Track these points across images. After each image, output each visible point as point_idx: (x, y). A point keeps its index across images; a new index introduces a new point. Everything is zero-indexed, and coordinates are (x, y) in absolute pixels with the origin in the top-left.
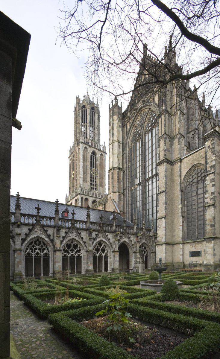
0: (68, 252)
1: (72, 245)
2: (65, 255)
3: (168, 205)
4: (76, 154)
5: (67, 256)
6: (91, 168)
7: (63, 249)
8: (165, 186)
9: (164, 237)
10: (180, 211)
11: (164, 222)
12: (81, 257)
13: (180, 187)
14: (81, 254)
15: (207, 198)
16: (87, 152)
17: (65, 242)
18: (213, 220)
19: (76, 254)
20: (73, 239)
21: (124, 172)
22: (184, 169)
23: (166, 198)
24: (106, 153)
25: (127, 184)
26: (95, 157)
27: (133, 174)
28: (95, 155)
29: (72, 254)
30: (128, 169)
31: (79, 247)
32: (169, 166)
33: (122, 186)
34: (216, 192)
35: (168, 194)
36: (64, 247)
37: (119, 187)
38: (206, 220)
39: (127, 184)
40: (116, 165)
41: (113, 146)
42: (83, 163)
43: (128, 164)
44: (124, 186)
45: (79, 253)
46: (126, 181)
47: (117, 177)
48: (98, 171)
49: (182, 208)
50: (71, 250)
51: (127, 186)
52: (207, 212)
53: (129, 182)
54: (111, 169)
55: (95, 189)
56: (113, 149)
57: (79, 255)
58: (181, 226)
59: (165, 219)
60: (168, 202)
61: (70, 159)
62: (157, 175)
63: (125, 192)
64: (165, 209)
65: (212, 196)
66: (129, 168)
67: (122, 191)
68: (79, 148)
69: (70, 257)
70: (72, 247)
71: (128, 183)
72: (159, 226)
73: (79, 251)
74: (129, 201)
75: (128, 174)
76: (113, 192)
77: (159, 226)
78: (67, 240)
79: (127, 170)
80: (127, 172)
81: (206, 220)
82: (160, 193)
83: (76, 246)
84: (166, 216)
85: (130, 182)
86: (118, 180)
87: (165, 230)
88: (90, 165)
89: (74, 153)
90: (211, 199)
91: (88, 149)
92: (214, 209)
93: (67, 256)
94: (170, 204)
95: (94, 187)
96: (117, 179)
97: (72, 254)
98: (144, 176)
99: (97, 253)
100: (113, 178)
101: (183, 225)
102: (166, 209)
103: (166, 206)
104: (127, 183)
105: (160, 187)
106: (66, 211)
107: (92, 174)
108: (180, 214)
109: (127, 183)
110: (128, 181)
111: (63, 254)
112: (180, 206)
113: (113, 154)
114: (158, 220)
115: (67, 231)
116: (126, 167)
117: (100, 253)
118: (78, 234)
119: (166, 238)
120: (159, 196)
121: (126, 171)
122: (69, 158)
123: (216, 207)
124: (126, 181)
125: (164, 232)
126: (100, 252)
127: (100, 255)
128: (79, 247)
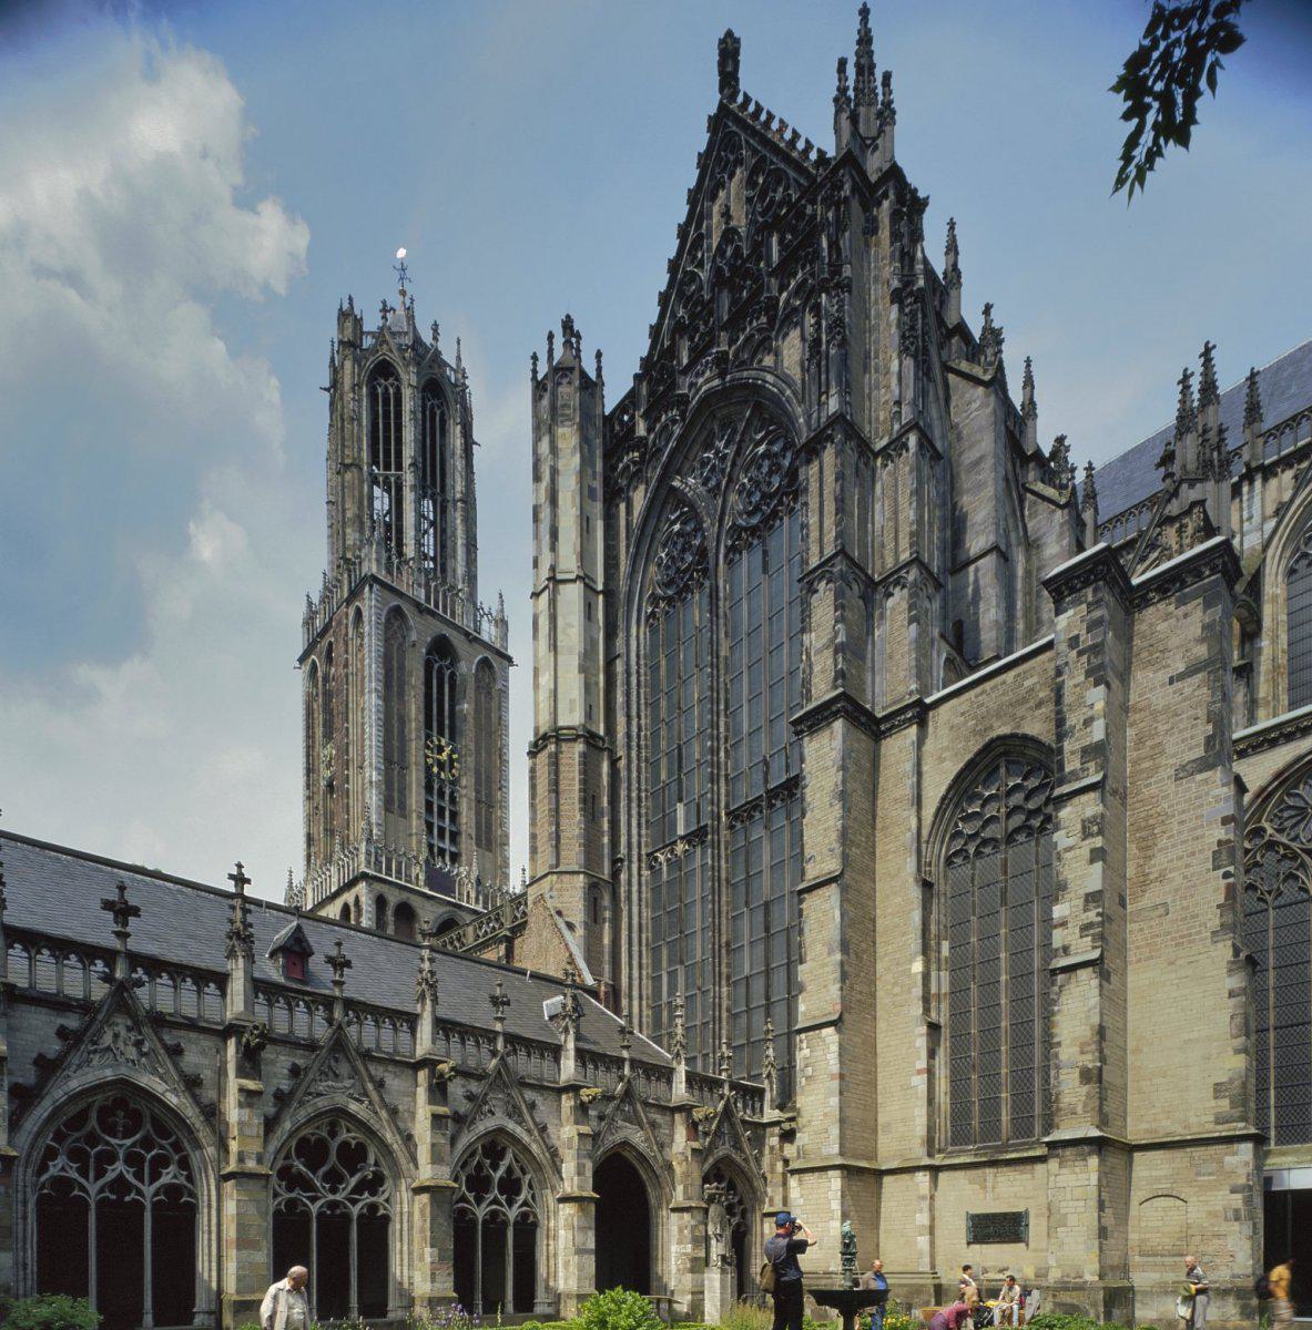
0: (308, 1186)
1: (334, 1145)
2: (291, 1204)
3: (853, 956)
5: (301, 1208)
7: (279, 1164)
8: (838, 851)
9: (835, 1131)
10: (918, 991)
11: (834, 1048)
13: (919, 861)
14: (387, 1201)
15: (1064, 924)
17: (287, 1125)
18: (1093, 1047)
19: (354, 1202)
21: (614, 762)
22: (941, 760)
29: (331, 1197)
30: (639, 746)
31: (376, 1164)
33: (606, 840)
34: (1107, 895)
36: (287, 1157)
38: (1059, 1044)
40: (572, 717)
44: (614, 844)
45: (373, 1193)
47: (577, 787)
49: (926, 976)
50: (326, 1178)
52: (1063, 999)
54: (545, 737)
56: (553, 618)
57: (373, 1207)
58: (919, 1072)
59: (839, 1031)
62: (791, 789)
63: (623, 877)
65: (1092, 916)
69: (320, 1215)
70: (333, 1158)
72: (809, 1071)
73: (374, 1184)
74: (640, 924)
76: (555, 870)
77: (809, 1071)
78: (302, 1115)
79: (634, 754)
81: (1059, 1044)
82: (810, 890)
83: (353, 1156)
84: (846, 1016)
86: (584, 801)
87: (841, 1093)
90: (1085, 928)
92: (1101, 985)
94: (864, 951)
96: (576, 795)
97: (331, 1197)
98: (723, 791)
99: (479, 1200)
101: (930, 1071)
102: (844, 976)
103: (845, 957)
104: (634, 822)
105: (813, 852)
109: (634, 822)
111: (276, 1195)
112: (918, 967)
113: (554, 647)
114: (803, 1036)
115: (300, 1062)
116: (628, 735)
117: (495, 1201)
118: (370, 1086)
119: (842, 1137)
120: (804, 906)
123: (1109, 974)
125: (834, 1101)
126: (490, 1197)
127: (494, 1214)
128: (371, 1160)
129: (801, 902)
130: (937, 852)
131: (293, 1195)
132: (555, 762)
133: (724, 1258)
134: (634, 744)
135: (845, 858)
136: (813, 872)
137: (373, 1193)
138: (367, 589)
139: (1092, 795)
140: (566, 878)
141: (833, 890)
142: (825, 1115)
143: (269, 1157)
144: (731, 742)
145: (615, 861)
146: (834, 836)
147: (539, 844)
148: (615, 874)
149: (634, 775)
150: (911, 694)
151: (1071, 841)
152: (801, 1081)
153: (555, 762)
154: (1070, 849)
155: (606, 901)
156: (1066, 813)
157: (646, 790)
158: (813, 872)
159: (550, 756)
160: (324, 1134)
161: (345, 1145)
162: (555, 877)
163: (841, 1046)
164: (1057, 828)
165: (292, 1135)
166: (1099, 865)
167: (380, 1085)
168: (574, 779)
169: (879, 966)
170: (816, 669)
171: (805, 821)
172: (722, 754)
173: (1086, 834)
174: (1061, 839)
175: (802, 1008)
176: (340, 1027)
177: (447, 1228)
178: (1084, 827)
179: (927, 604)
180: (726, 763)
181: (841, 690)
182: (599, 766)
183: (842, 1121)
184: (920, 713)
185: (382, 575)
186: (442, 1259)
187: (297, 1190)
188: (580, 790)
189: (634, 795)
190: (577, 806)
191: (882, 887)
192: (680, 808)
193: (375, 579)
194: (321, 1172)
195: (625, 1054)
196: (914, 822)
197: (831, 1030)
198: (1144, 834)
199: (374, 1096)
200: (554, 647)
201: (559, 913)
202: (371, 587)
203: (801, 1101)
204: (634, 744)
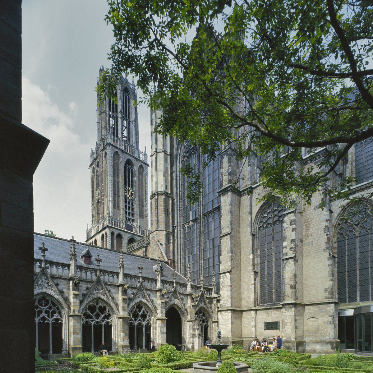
0: (91, 318)
1: (98, 307)
2: (87, 322)
5: (89, 323)
7: (83, 313)
8: (230, 227)
9: (230, 300)
10: (251, 263)
11: (229, 278)
12: (111, 325)
14: (112, 321)
15: (286, 247)
17: (86, 302)
18: (293, 279)
19: (103, 321)
20: (100, 298)
21: (173, 200)
23: (231, 244)
30: (180, 196)
31: (109, 311)
33: (171, 221)
34: (297, 240)
35: (234, 238)
38: (285, 278)
40: (161, 189)
41: (156, 158)
46: (177, 214)
47: (163, 207)
49: (253, 259)
50: (96, 315)
51: (179, 221)
52: (286, 267)
54: (154, 194)
56: (156, 162)
57: (108, 323)
58: (252, 284)
59: (230, 274)
60: (234, 249)
63: (176, 231)
64: (230, 259)
65: (293, 245)
69: (94, 325)
71: (180, 217)
72: (223, 284)
73: (108, 317)
76: (157, 230)
77: (223, 284)
78: (89, 299)
79: (178, 198)
80: (177, 200)
81: (285, 278)
83: (103, 309)
84: (232, 270)
86: (165, 211)
87: (231, 290)
90: (291, 248)
92: (295, 263)
93: (89, 323)
94: (237, 253)
96: (163, 210)
97: (97, 320)
98: (202, 209)
99: (136, 320)
100: (157, 208)
101: (255, 284)
102: (232, 260)
106: (88, 256)
108: (251, 268)
110: (180, 214)
111: (83, 320)
112: (251, 257)
113: (157, 170)
115: (89, 286)
116: (177, 193)
117: (140, 320)
118: (107, 292)
120: (221, 241)
123: (297, 260)
124: (177, 214)
125: (229, 292)
126: (138, 319)
127: (140, 324)
128: (107, 310)
129: (221, 240)
130: (256, 226)
131: (87, 320)
132: (157, 201)
133: (199, 334)
134: (178, 195)
135: (232, 229)
136: (224, 231)
137: (108, 319)
139: (292, 214)
140: (160, 232)
141: (228, 237)
142: (227, 296)
143: (81, 311)
144: (203, 195)
145: (173, 227)
146: (229, 222)
148: (173, 230)
149: (179, 203)
150: (249, 185)
151: (287, 226)
152: (221, 287)
153: (157, 201)
154: (287, 228)
155: (171, 238)
156: (286, 219)
158: (224, 231)
159: (156, 199)
160: (95, 304)
161: (100, 307)
162: (157, 232)
163: (231, 278)
164: (284, 223)
165: (87, 305)
166: (294, 232)
167: (109, 291)
169: (242, 256)
170: (224, 178)
172: (201, 199)
173: (291, 224)
174: (285, 225)
175: (221, 268)
176: (99, 277)
177: (127, 327)
178: (290, 223)
179: (253, 161)
181: (230, 184)
182: (169, 202)
183: (231, 298)
184: (250, 191)
186: (125, 336)
187: (88, 319)
189: (178, 209)
191: (242, 235)
192: (191, 213)
194: (95, 313)
195: (174, 281)
197: (228, 274)
198: (307, 223)
199: (108, 294)
200: (157, 170)
201: (158, 241)
203: (221, 292)
204: (178, 195)
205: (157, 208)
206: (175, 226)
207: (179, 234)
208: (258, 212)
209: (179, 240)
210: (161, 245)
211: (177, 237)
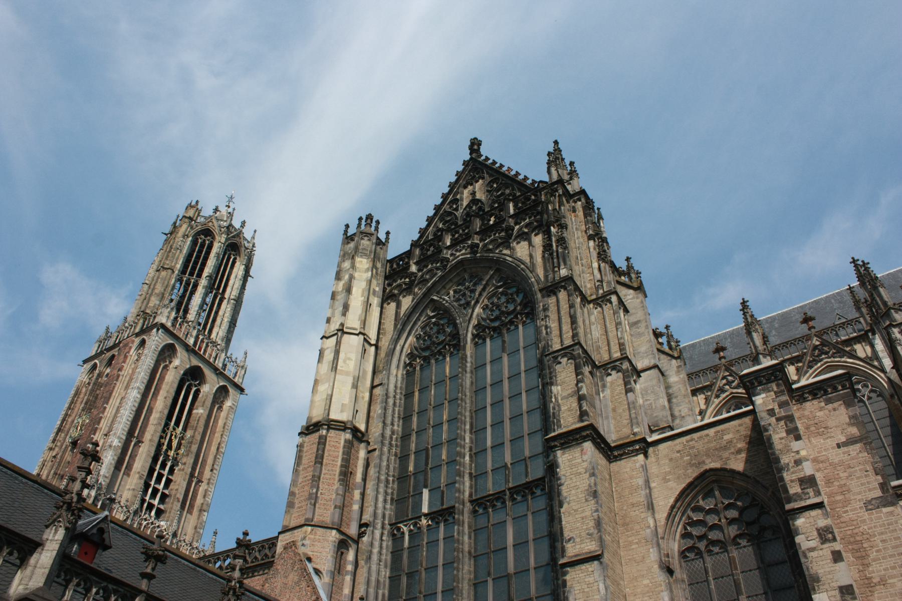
4: (122, 357)
6: (167, 425)
16: (170, 362)
22: (666, 480)
24: (242, 390)
25: (380, 505)
26: (194, 389)
27: (411, 468)
28: (199, 384)
30: (390, 444)
32: (602, 461)
33: (356, 507)
37: (343, 507)
39: (380, 505)
42: (139, 396)
43: (392, 424)
48: (191, 443)
51: (380, 512)
53: (389, 498)
55: (159, 513)
61: (88, 366)
66: (394, 443)
67: (353, 530)
68: (143, 342)
71: (385, 501)
74: (378, 581)
75: (387, 462)
79: (385, 449)
80: (381, 454)
85: (392, 499)
88: (166, 412)
89: (115, 352)
91: (179, 354)
95: (156, 502)
104: (381, 498)
105: (571, 535)
107: (165, 447)
109: (381, 498)
110: (386, 493)
121: (381, 450)
122: (85, 362)
134: (387, 442)
138: (155, 330)
144: (474, 451)
147: (296, 501)
149: (385, 463)
153: (322, 442)
157: (394, 476)
162: (310, 528)
168: (337, 457)
171: (562, 510)
180: (471, 465)
182: (357, 452)
185: (169, 324)
188: (342, 466)
190: (337, 477)
192: (426, 493)
193: (163, 326)
196: (651, 522)
201: (309, 559)
202: (158, 330)
205: (319, 459)
206: (366, 525)
207: (376, 550)
208: (673, 507)
209: (374, 567)
210: (317, 572)
211: (369, 558)
